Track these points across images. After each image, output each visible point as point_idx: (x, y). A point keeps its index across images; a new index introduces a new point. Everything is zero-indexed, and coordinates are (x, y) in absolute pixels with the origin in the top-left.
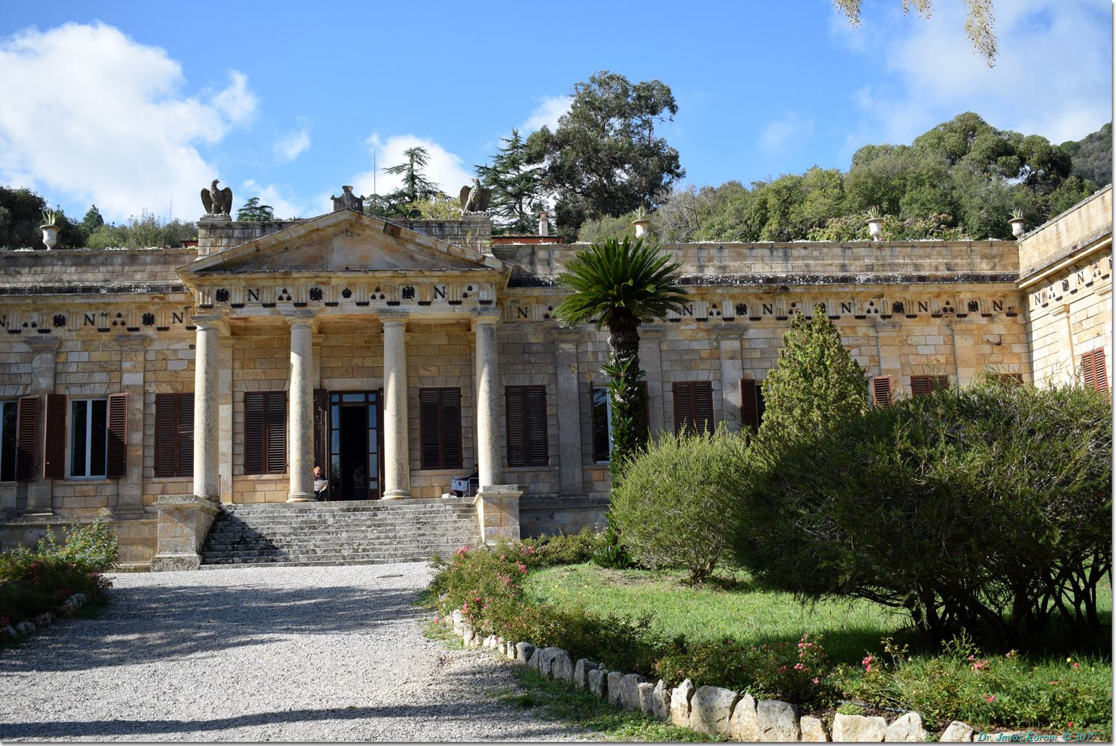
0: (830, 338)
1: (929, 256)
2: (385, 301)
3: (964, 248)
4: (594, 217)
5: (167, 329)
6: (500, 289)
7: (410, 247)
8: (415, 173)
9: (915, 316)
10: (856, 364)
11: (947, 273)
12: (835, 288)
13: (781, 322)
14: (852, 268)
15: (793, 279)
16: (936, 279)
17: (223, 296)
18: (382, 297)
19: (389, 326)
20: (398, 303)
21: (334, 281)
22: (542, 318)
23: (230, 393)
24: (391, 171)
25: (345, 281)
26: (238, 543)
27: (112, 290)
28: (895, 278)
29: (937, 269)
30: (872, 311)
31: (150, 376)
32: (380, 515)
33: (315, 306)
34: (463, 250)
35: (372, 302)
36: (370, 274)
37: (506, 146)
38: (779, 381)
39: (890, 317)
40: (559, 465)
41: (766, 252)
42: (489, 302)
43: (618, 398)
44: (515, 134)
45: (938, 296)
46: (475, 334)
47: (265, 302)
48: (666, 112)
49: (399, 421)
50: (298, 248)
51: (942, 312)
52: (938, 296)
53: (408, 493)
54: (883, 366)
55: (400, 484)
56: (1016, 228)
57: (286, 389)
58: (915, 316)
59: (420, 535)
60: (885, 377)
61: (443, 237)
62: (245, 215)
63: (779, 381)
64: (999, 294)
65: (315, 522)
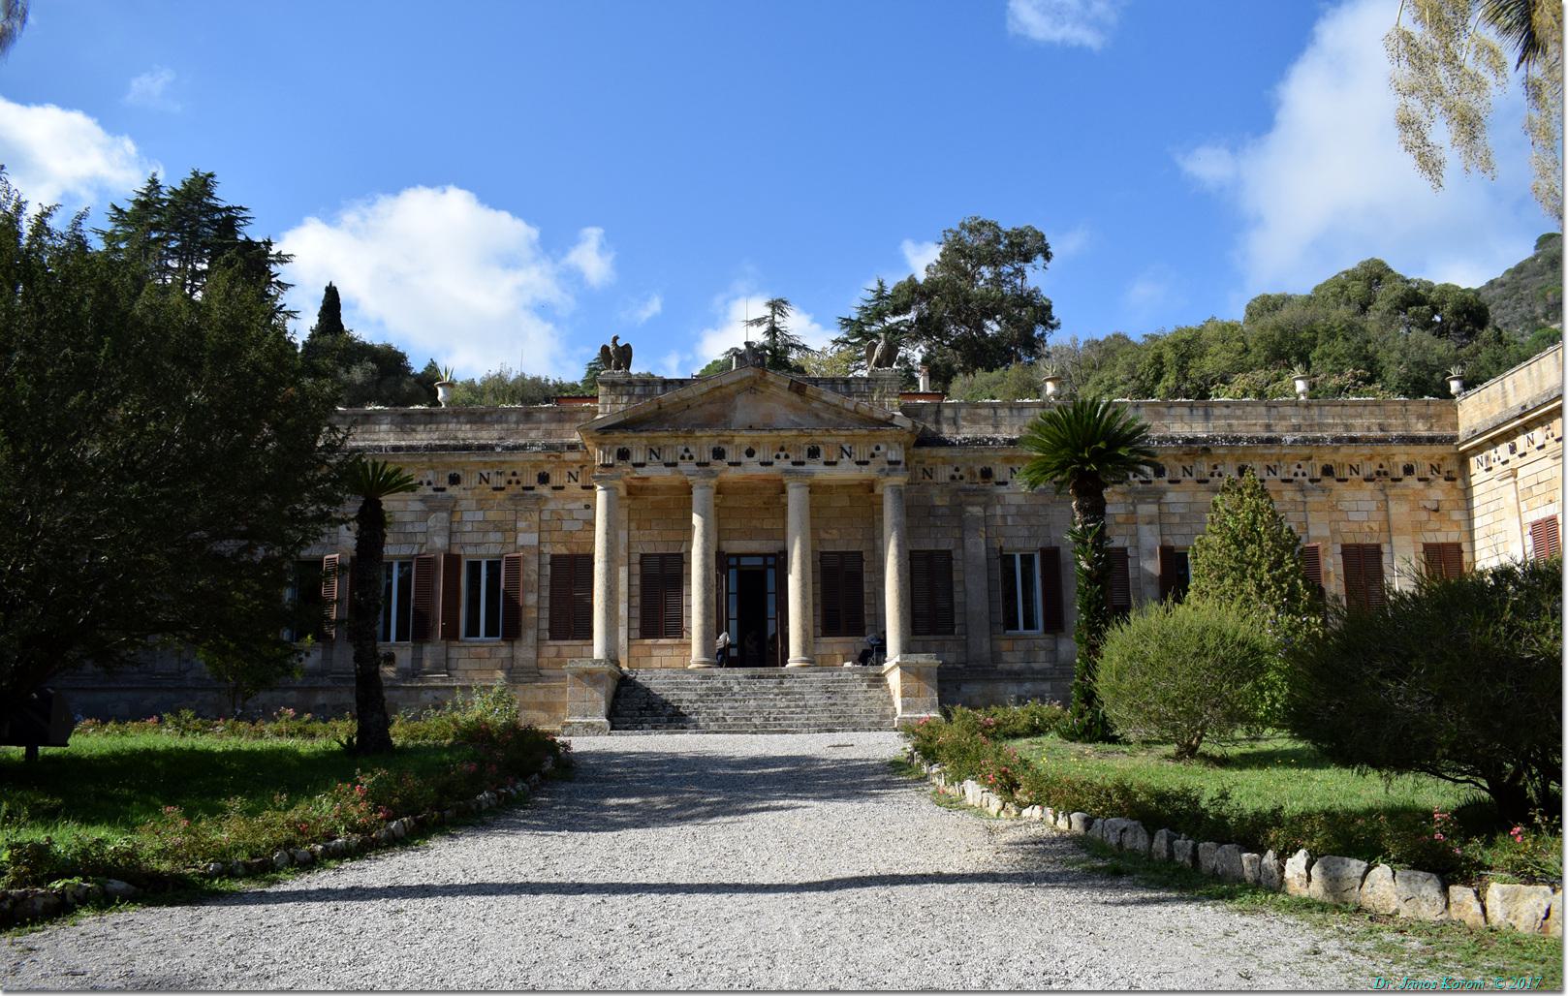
0: (1263, 503)
1: (1360, 416)
2: (789, 461)
3: (1398, 408)
4: (965, 370)
5: (562, 488)
6: (907, 449)
7: (815, 404)
8: (777, 325)
9: (1346, 480)
10: (1290, 530)
11: (1380, 434)
12: (1261, 449)
13: (1202, 485)
14: (1278, 428)
15: (1214, 439)
16: (1368, 441)
17: (624, 455)
18: (787, 457)
19: (793, 487)
20: (802, 463)
21: (737, 440)
22: (948, 480)
23: (626, 554)
24: (751, 323)
25: (749, 440)
26: (645, 709)
27: (507, 448)
28: (1323, 438)
29: (1369, 429)
30: (1300, 474)
31: (545, 535)
32: (787, 684)
33: (718, 466)
34: (871, 409)
35: (776, 462)
36: (775, 433)
37: (871, 296)
38: (1207, 548)
39: (1318, 480)
40: (966, 634)
41: (1186, 411)
42: (898, 463)
43: (1084, 565)
44: (881, 284)
45: (1371, 458)
46: (881, 496)
47: (666, 461)
48: (1040, 259)
49: (804, 586)
50: (700, 406)
51: (1375, 476)
52: (1371, 458)
53: (812, 660)
54: (1311, 533)
55: (805, 650)
56: (1455, 386)
57: (683, 551)
58: (1346, 480)
59: (831, 705)
60: (1314, 545)
61: (850, 395)
62: (595, 369)
63: (1207, 548)
64: (1437, 457)
65: (720, 689)
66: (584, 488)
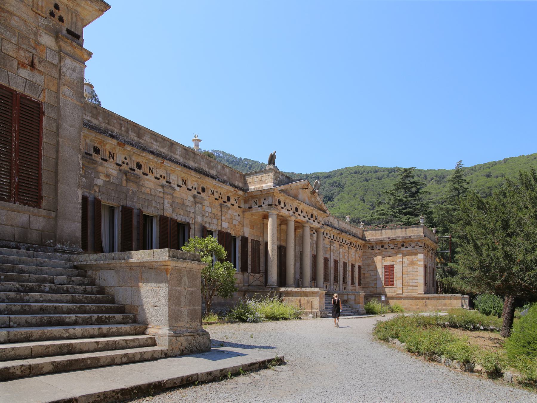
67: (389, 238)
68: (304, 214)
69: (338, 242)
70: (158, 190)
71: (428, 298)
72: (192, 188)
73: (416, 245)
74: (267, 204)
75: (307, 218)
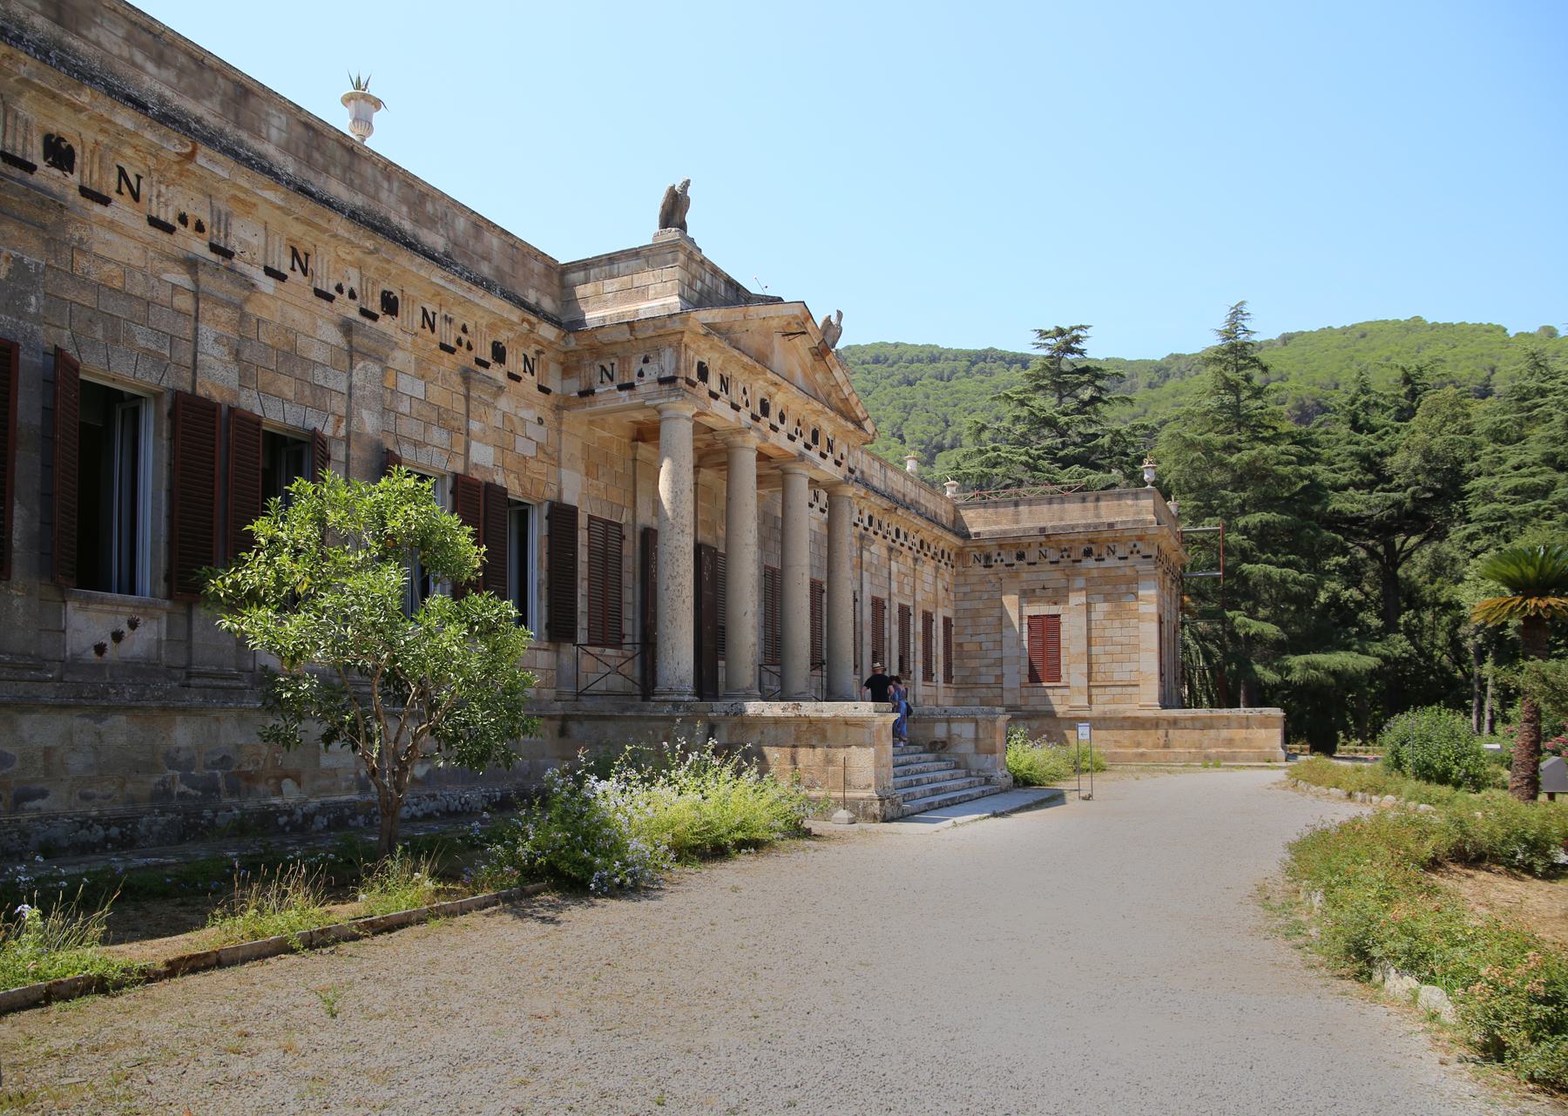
66: (541, 388)
67: (1042, 530)
68: (788, 427)
69: (885, 537)
70: (165, 277)
71: (1174, 723)
72: (339, 289)
73: (1132, 553)
74: (654, 377)
75: (799, 443)
